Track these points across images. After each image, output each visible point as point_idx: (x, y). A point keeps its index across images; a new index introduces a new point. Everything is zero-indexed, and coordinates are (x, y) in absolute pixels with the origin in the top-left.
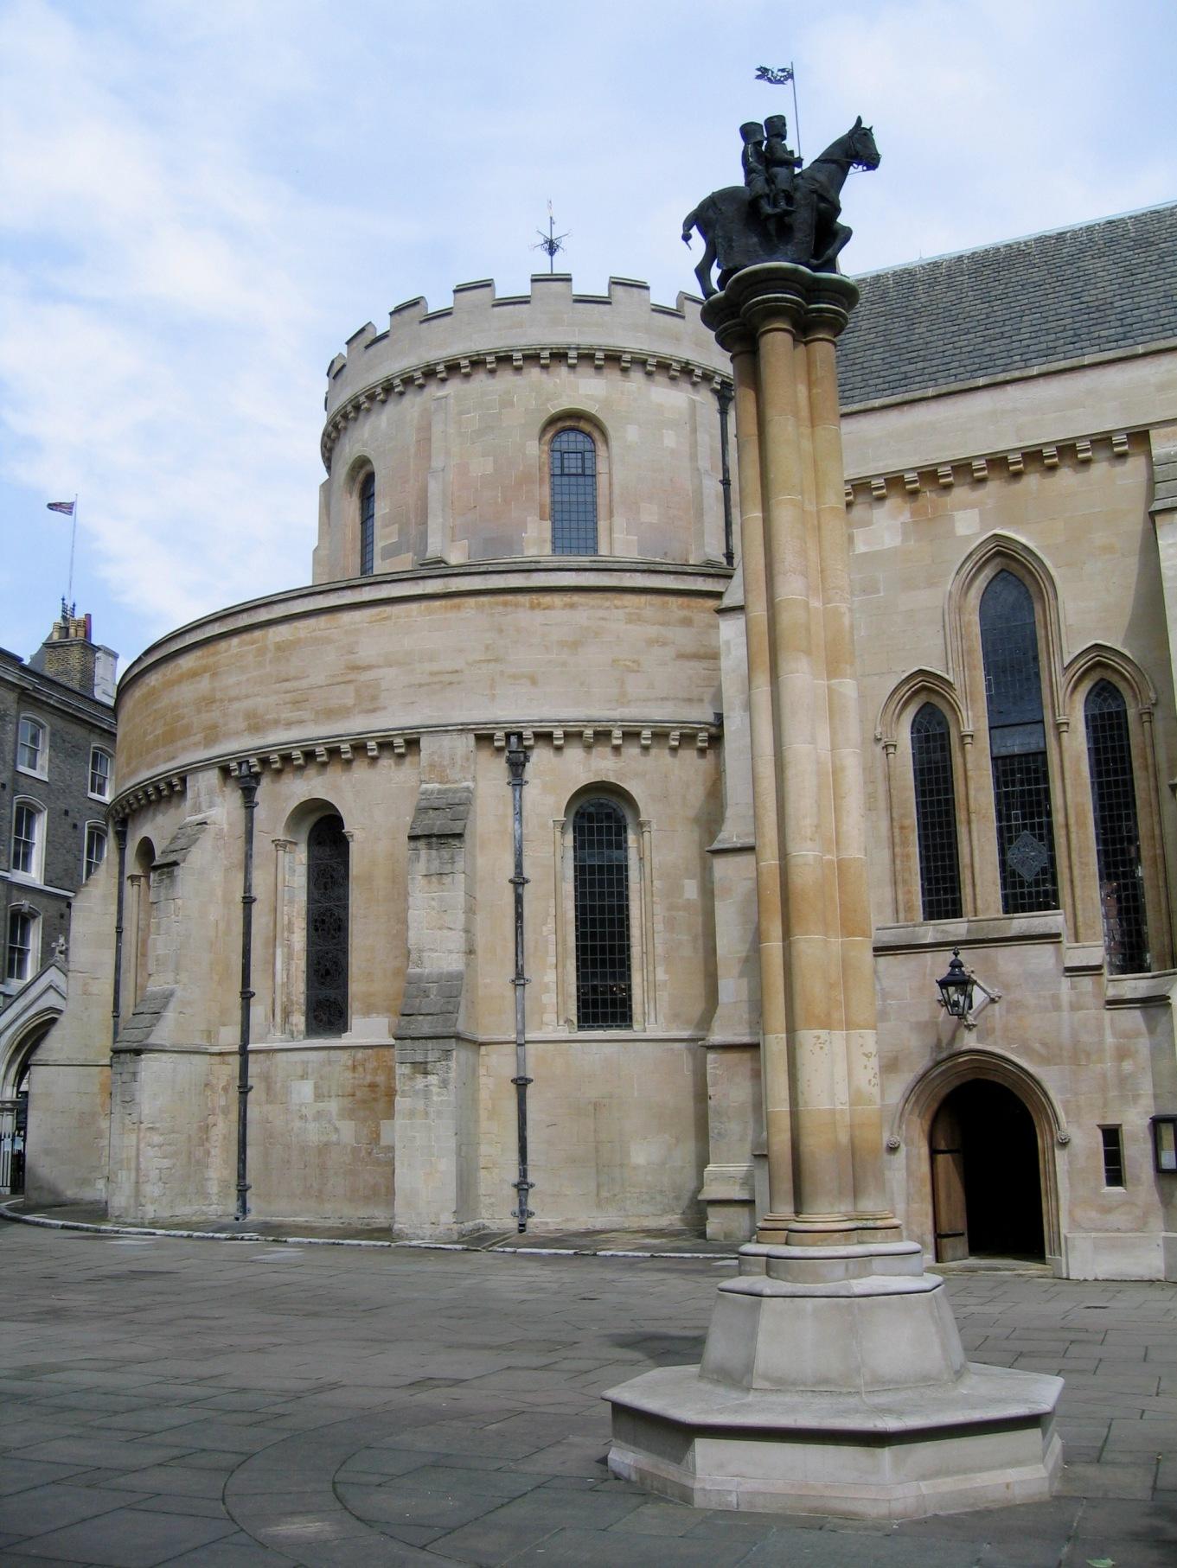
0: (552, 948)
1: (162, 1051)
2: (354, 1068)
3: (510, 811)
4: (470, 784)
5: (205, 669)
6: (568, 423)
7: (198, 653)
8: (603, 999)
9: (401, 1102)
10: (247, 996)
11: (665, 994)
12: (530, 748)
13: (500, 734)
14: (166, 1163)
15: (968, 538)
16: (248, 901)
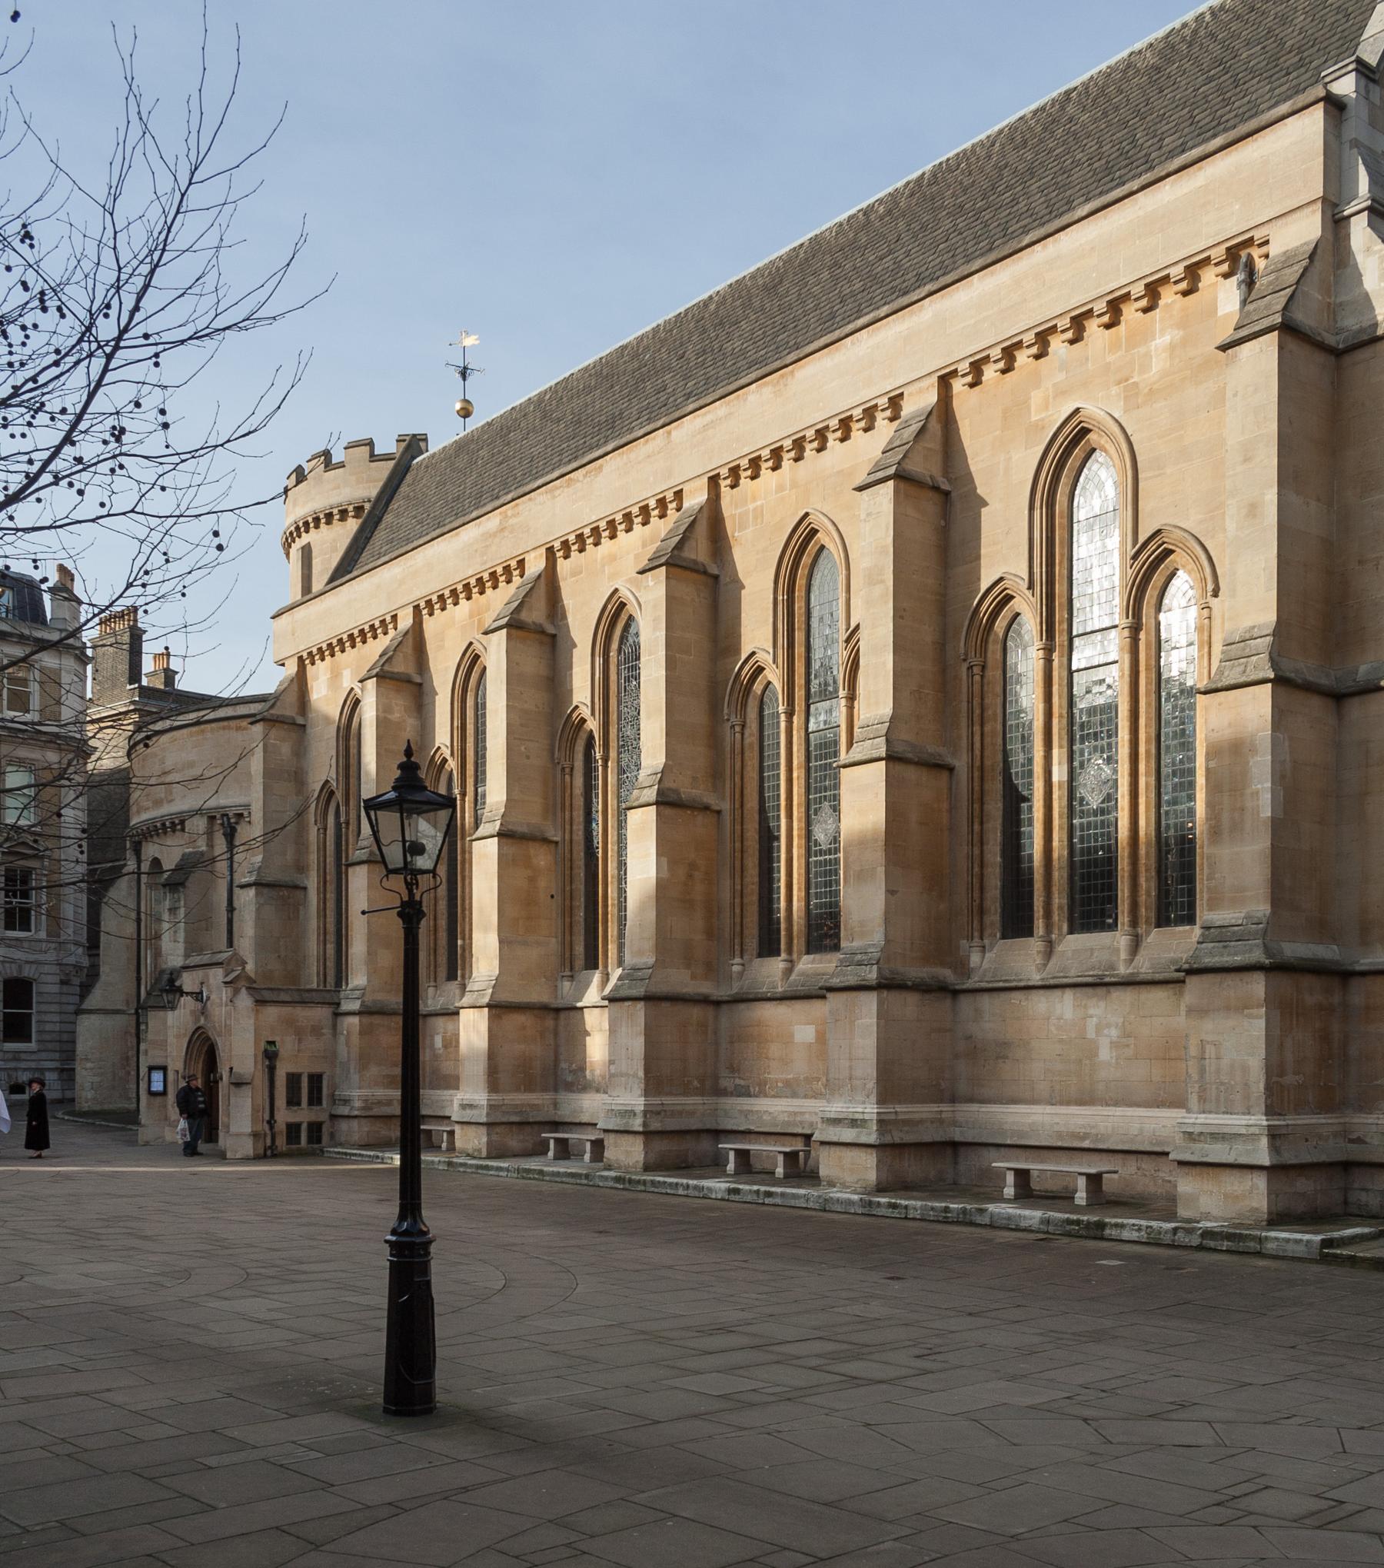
4: (204, 848)
14: (97, 1079)
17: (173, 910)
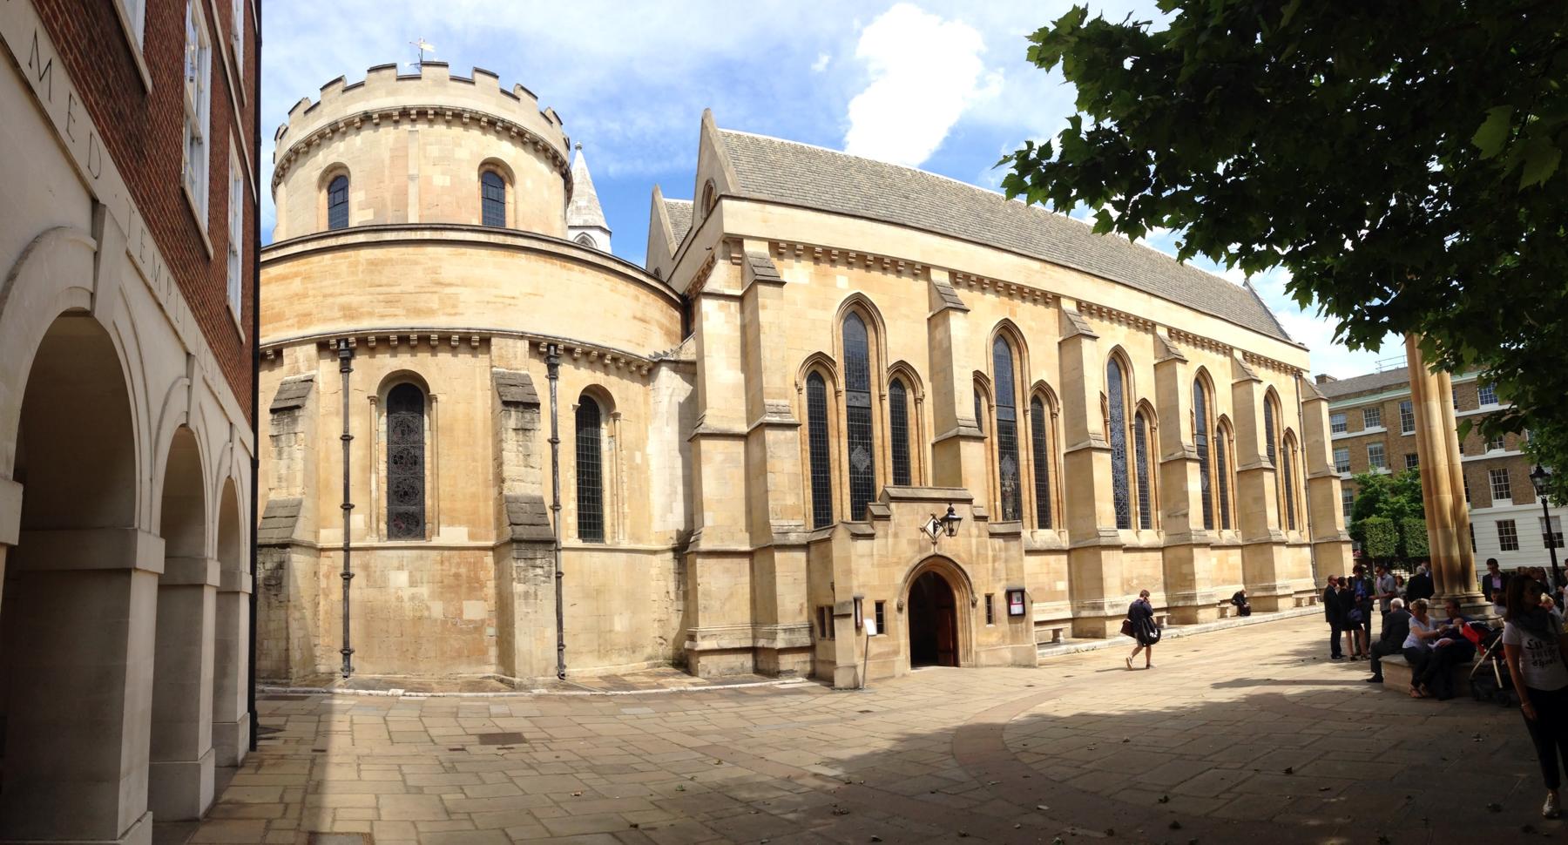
10: (347, 507)
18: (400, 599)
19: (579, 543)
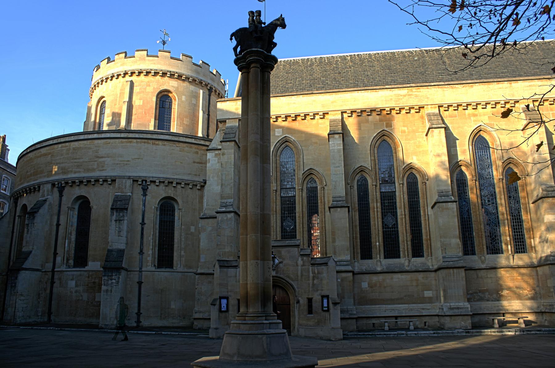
0: (151, 244)
1: (26, 269)
2: (89, 277)
3: (142, 203)
4: (130, 194)
5: (50, 154)
6: (166, 93)
7: (47, 148)
8: (165, 259)
9: (104, 288)
11: (184, 259)
12: (149, 185)
13: (140, 180)
15: (278, 137)
16: (58, 225)
17: (118, 221)
18: (71, 292)
19: (153, 269)
